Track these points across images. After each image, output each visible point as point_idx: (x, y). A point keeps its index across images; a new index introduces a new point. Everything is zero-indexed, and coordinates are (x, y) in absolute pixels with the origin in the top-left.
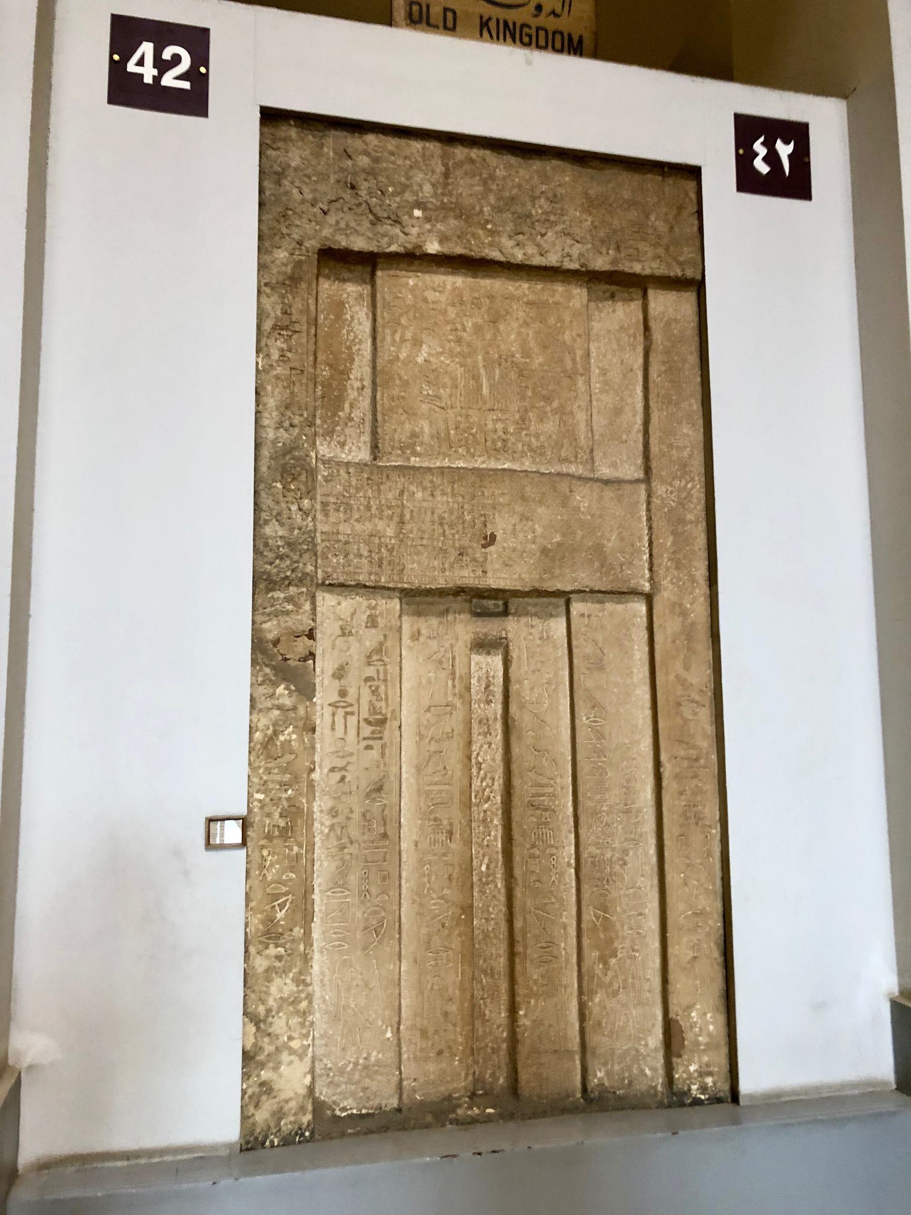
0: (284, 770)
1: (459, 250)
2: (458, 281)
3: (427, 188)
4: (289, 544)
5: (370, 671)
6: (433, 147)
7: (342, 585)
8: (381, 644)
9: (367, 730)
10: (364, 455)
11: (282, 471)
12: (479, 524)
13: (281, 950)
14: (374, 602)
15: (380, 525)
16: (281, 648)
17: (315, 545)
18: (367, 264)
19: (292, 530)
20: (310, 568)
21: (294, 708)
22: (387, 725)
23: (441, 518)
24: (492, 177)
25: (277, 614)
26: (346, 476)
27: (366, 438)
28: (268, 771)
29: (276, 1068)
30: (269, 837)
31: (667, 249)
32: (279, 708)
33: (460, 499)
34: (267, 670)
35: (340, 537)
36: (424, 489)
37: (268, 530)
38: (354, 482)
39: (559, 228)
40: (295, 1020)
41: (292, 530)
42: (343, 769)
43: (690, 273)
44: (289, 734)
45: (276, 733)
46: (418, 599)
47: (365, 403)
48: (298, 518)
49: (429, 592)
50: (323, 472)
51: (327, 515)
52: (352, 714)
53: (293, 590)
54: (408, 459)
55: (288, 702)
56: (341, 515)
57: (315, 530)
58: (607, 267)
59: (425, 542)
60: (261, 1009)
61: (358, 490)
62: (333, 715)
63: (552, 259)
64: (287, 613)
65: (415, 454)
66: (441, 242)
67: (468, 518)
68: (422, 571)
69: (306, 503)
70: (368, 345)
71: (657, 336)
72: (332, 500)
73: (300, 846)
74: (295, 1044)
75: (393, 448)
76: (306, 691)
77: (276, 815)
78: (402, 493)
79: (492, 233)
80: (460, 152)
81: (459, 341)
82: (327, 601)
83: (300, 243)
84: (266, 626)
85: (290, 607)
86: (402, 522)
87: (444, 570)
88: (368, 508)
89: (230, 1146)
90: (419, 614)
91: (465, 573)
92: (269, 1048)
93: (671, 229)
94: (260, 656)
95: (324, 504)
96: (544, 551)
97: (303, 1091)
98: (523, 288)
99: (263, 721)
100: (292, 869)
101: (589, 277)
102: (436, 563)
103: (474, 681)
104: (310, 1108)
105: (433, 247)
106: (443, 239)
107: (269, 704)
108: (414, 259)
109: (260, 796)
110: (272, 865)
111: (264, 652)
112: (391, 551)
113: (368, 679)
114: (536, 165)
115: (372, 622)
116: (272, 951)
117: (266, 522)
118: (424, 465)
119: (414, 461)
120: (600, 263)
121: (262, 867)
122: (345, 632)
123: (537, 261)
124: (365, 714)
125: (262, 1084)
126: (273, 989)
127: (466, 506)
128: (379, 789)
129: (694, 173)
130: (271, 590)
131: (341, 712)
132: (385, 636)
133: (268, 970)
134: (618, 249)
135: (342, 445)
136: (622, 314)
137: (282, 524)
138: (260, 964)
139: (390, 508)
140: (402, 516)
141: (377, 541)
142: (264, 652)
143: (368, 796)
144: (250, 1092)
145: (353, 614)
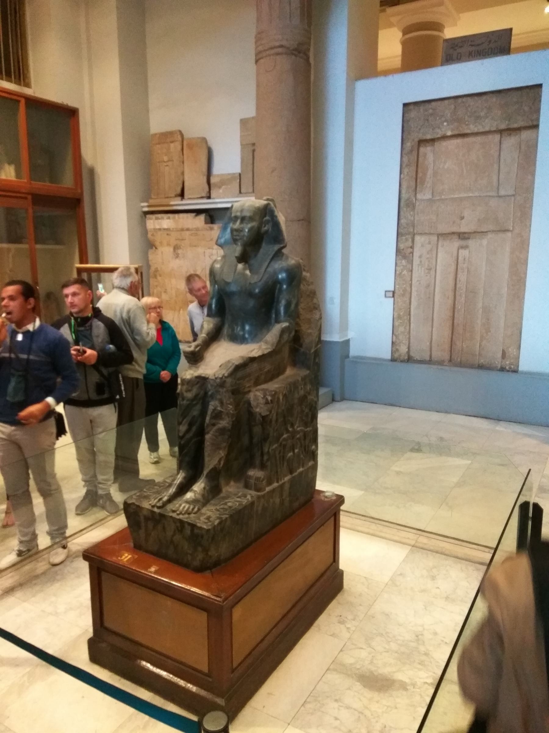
1: (456, 132)
2: (459, 141)
3: (449, 115)
5: (428, 256)
6: (451, 101)
9: (427, 271)
11: (405, 205)
18: (433, 141)
24: (469, 106)
27: (431, 191)
31: (527, 117)
39: (490, 117)
43: (535, 123)
44: (405, 272)
46: (441, 236)
48: (410, 217)
50: (417, 204)
53: (407, 236)
57: (414, 219)
58: (506, 128)
63: (487, 129)
66: (452, 132)
68: (443, 228)
69: (412, 213)
70: (432, 165)
71: (523, 147)
77: (401, 291)
79: (467, 125)
80: (460, 100)
83: (413, 140)
93: (531, 108)
96: (479, 220)
98: (479, 139)
101: (501, 132)
103: (460, 258)
105: (449, 133)
106: (452, 130)
108: (444, 138)
113: (427, 258)
114: (484, 97)
119: (443, 197)
120: (503, 126)
121: (398, 302)
122: (422, 246)
123: (482, 130)
129: (540, 86)
133: (399, 325)
134: (509, 121)
135: (424, 195)
136: (510, 142)
142: (400, 252)
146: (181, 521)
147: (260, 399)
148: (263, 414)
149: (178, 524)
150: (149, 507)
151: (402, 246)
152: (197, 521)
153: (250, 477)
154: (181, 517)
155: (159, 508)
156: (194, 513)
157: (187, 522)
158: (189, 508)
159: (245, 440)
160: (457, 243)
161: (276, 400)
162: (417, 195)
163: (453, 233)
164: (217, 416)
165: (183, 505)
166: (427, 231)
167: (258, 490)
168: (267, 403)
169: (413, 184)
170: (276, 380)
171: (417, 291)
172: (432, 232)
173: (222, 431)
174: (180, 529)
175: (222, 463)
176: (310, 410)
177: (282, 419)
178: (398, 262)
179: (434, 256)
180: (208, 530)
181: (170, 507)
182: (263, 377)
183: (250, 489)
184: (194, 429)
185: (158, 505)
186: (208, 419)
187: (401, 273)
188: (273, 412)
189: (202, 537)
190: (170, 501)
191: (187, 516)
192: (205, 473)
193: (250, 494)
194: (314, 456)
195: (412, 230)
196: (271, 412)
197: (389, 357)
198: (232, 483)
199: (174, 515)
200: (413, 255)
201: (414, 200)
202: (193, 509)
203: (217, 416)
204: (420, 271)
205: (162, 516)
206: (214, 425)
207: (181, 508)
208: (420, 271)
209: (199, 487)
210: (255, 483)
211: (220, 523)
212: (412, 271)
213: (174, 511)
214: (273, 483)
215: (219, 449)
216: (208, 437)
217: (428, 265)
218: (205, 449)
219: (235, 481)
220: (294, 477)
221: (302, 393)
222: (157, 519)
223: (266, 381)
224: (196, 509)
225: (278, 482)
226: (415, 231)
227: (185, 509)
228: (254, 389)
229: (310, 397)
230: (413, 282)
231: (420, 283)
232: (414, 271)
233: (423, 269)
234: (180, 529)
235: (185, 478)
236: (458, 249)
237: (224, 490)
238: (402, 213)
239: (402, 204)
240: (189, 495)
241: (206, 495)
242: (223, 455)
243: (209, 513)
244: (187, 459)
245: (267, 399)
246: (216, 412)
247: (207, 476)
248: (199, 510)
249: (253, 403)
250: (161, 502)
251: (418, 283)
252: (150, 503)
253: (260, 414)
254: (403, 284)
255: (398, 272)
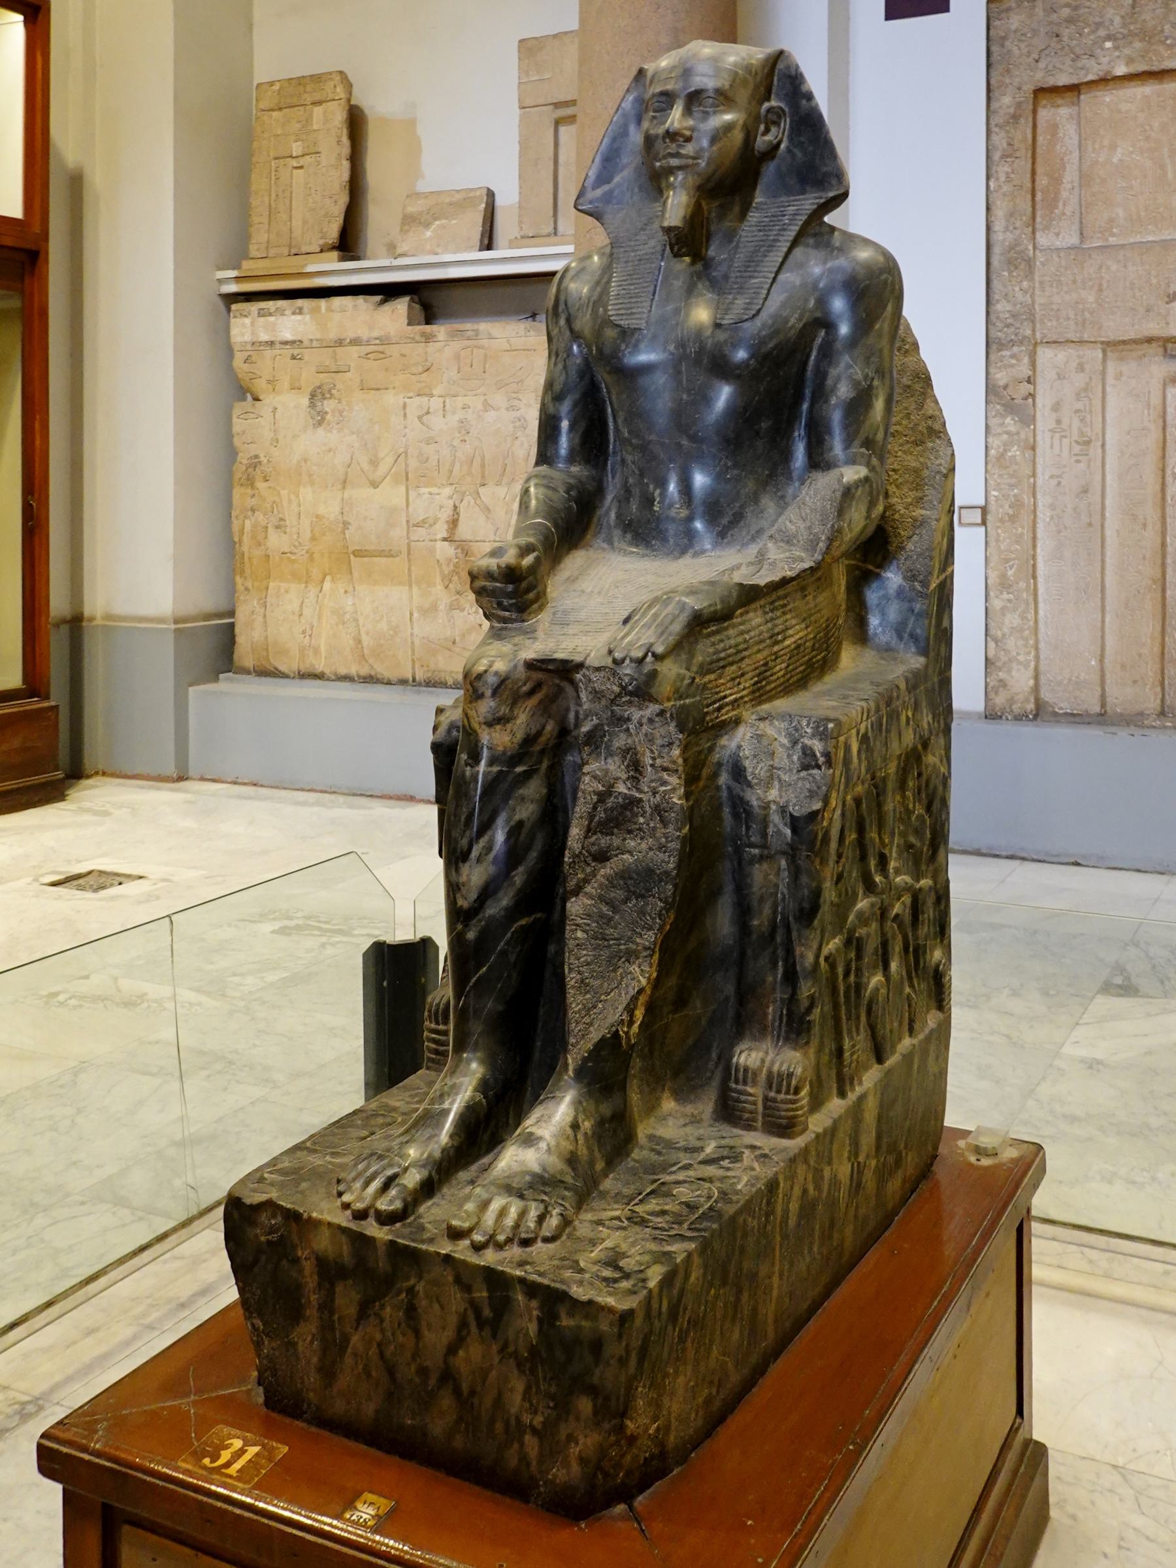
0: (1011, 476)
4: (1013, 316)
5: (1079, 405)
7: (1055, 342)
8: (1087, 384)
9: (1077, 449)
10: (1074, 240)
12: (1163, 287)
13: (1011, 596)
14: (1081, 353)
15: (1083, 293)
16: (1010, 390)
17: (1033, 315)
19: (1015, 305)
20: (1028, 332)
21: (1018, 433)
22: (1092, 445)
23: (1132, 284)
25: (1005, 367)
26: (1057, 259)
28: (1001, 476)
29: (1009, 671)
30: (1002, 521)
32: (1007, 433)
33: (1147, 267)
34: (998, 407)
35: (1055, 307)
36: (1119, 262)
37: (999, 307)
38: (1063, 263)
40: (1020, 643)
41: (1015, 305)
42: (1058, 477)
44: (1015, 451)
45: (1005, 450)
47: (1074, 201)
49: (1124, 342)
50: (1040, 257)
51: (1043, 291)
52: (1065, 437)
53: (1015, 349)
54: (1107, 240)
55: (1012, 429)
56: (1055, 290)
59: (1119, 304)
60: (999, 633)
61: (1066, 268)
62: (1052, 438)
64: (1012, 366)
65: (1113, 235)
67: (1154, 281)
68: (1117, 326)
69: (1025, 284)
72: (1047, 278)
73: (1023, 528)
74: (1021, 658)
75: (1094, 232)
76: (1028, 420)
78: (1101, 267)
81: (1147, 138)
82: (1045, 355)
84: (998, 376)
85: (1014, 361)
86: (1100, 290)
87: (1133, 325)
88: (1074, 282)
89: (979, 714)
90: (1121, 359)
91: (1151, 325)
92: (1004, 659)
94: (992, 398)
95: (1041, 283)
97: (1027, 689)
99: (995, 442)
100: (1017, 542)
102: (1127, 320)
104: (1032, 700)
107: (999, 430)
109: (996, 493)
110: (1004, 539)
111: (996, 394)
112: (1091, 313)
113: (1077, 411)
115: (1081, 368)
116: (1005, 596)
117: (998, 301)
118: (1121, 242)
119: (1112, 240)
121: (997, 541)
122: (1060, 377)
124: (1075, 436)
125: (1001, 681)
126: (1007, 621)
127: (1153, 272)
128: (1086, 491)
130: (1000, 350)
131: (1057, 435)
132: (1090, 378)
135: (1057, 235)
137: (1009, 301)
138: (997, 604)
139: (1090, 280)
140: (1100, 285)
141: (1081, 306)
142: (996, 394)
143: (1077, 496)
144: (992, 684)
145: (1067, 362)
146: (493, 1277)
147: (781, 753)
148: (797, 811)
149: (481, 1294)
150: (343, 1219)
151: (1001, 377)
152: (568, 1274)
153: (748, 1075)
154: (490, 1257)
155: (386, 1219)
156: (546, 1240)
157: (522, 1281)
158: (523, 1214)
159: (722, 922)
160: (1158, 368)
161: (841, 754)
162: (1038, 235)
163: (1149, 340)
164: (617, 817)
165: (496, 1205)
166: (1071, 336)
167: (784, 1128)
168: (808, 762)
169: (1025, 205)
170: (817, 687)
171: (1052, 507)
172: (1086, 337)
173: (638, 882)
174: (487, 1312)
175: (639, 1014)
176: (928, 809)
177: (854, 836)
178: (994, 422)
179: (1097, 403)
180: (626, 1317)
181: (432, 1212)
182: (780, 668)
183: (749, 1127)
184: (519, 877)
185: (383, 1205)
186: (575, 832)
187: (1002, 455)
188: (833, 803)
189: (597, 1346)
190: (428, 1188)
191: (515, 1251)
192: (572, 1060)
193: (753, 1147)
194: (938, 989)
195: (1028, 332)
196: (826, 801)
197: (980, 707)
198: (669, 1104)
199: (461, 1250)
200: (1034, 401)
201: (1031, 247)
202: (541, 1219)
203: (617, 817)
204: (1057, 450)
205: (405, 1257)
206: (602, 857)
207: (489, 1218)
208: (1057, 450)
209: (554, 1121)
210: (766, 1099)
211: (667, 1281)
212: (1033, 448)
213: (455, 1234)
214: (828, 1098)
215: (631, 956)
216: (575, 907)
217: (1082, 434)
218: (570, 960)
219: (680, 1096)
220: (889, 1073)
221: (909, 738)
222: (381, 1269)
223: (790, 687)
224: (553, 1221)
225: (842, 1094)
226: (1038, 336)
227: (509, 1221)
228: (749, 715)
229: (931, 759)
230: (1040, 482)
231: (1059, 484)
232: (1039, 451)
233: (1066, 441)
234: (487, 1312)
235: (484, 1086)
236: (1165, 385)
237: (643, 1131)
238: (996, 284)
239: (995, 261)
240: (514, 1158)
241: (583, 1151)
242: (644, 982)
243: (612, 1239)
244: (490, 1005)
245: (808, 752)
246: (610, 802)
247: (580, 1074)
248: (566, 1222)
249: (755, 769)
250: (393, 1192)
251: (1054, 482)
252: (346, 1198)
253: (783, 810)
254: (1012, 486)
255: (992, 452)
